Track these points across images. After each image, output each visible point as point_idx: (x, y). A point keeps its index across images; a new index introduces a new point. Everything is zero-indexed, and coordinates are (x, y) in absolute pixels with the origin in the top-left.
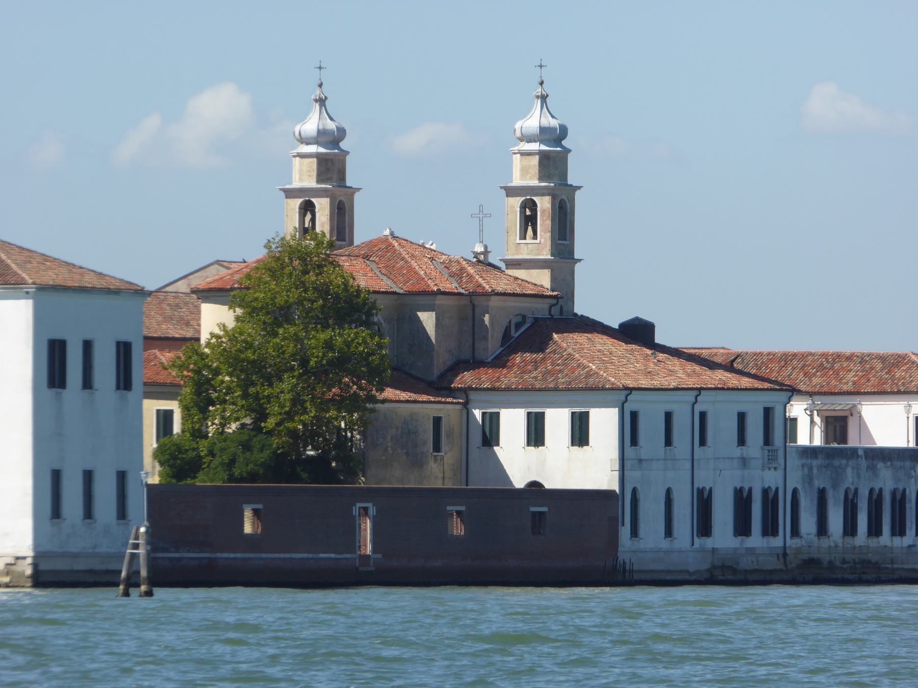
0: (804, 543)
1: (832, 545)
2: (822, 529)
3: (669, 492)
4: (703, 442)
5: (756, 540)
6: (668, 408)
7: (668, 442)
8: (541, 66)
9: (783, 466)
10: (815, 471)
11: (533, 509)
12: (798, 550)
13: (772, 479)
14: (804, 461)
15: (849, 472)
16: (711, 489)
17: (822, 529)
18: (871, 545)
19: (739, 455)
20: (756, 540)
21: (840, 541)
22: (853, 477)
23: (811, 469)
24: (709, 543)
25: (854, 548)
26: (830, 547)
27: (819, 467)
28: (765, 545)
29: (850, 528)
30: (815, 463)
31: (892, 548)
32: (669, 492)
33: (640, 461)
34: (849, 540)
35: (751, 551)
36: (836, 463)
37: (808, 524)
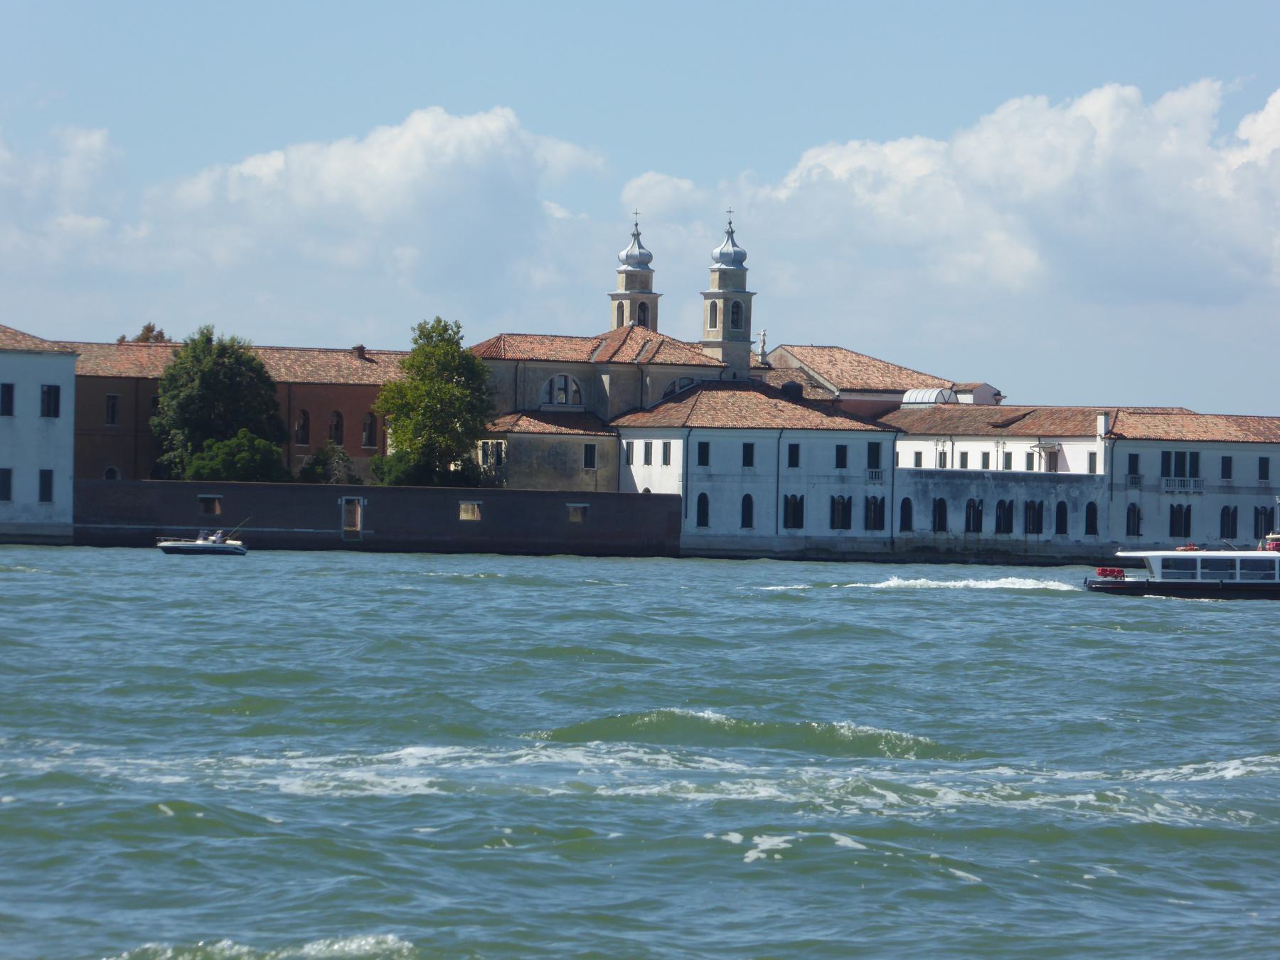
10: (931, 487)
12: (908, 541)
13: (876, 491)
21: (962, 536)
24: (800, 533)
30: (930, 481)
33: (710, 476)
35: (854, 539)
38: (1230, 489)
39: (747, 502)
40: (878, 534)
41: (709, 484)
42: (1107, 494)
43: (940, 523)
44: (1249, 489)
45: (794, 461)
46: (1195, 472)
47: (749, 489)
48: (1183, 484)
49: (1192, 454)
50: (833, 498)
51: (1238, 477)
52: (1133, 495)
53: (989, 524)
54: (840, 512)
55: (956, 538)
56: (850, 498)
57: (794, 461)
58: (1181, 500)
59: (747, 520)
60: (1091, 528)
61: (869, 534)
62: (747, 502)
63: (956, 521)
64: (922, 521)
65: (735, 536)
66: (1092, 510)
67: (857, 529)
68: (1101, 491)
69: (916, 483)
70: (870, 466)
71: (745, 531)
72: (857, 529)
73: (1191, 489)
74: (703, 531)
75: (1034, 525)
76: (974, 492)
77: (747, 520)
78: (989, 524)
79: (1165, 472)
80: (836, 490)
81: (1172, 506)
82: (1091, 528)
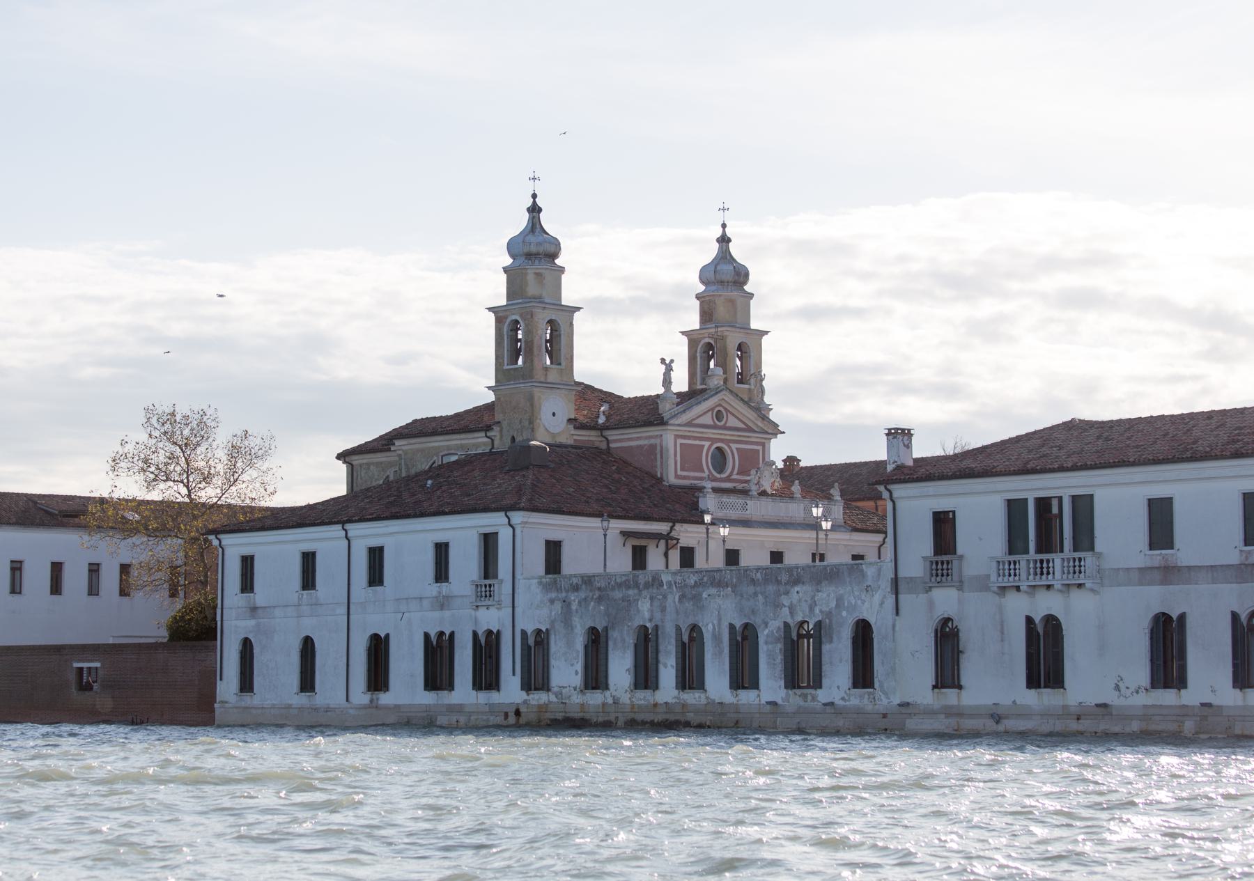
0: (553, 698)
1: (610, 701)
8: (534, 179)
10: (574, 607)
11: (76, 665)
13: (491, 618)
14: (553, 595)
19: (435, 594)
21: (625, 699)
23: (566, 603)
25: (655, 705)
26: (604, 704)
27: (584, 602)
30: (573, 597)
33: (254, 610)
36: (618, 594)
38: (1169, 574)
39: (308, 648)
40: (495, 697)
41: (253, 622)
42: (890, 600)
43: (595, 677)
44: (1215, 572)
45: (376, 577)
46: (1085, 537)
47: (308, 626)
48: (1043, 569)
49: (1075, 499)
50: (427, 636)
51: (1189, 546)
52: (946, 600)
53: (668, 674)
54: (438, 656)
55: (616, 702)
56: (452, 634)
57: (376, 577)
58: (1044, 605)
59: (307, 682)
60: (863, 676)
61: (483, 697)
62: (308, 648)
63: (620, 668)
64: (566, 672)
65: (289, 707)
66: (863, 634)
67: (463, 692)
68: (877, 597)
69: (552, 601)
70: (548, 572)
71: (303, 699)
72: (463, 692)
73: (1057, 579)
74: (247, 699)
75: (487, 677)
76: (644, 611)
77: (307, 682)
78: (668, 674)
79: (1015, 542)
80: (436, 622)
81: (1029, 620)
82: (863, 676)
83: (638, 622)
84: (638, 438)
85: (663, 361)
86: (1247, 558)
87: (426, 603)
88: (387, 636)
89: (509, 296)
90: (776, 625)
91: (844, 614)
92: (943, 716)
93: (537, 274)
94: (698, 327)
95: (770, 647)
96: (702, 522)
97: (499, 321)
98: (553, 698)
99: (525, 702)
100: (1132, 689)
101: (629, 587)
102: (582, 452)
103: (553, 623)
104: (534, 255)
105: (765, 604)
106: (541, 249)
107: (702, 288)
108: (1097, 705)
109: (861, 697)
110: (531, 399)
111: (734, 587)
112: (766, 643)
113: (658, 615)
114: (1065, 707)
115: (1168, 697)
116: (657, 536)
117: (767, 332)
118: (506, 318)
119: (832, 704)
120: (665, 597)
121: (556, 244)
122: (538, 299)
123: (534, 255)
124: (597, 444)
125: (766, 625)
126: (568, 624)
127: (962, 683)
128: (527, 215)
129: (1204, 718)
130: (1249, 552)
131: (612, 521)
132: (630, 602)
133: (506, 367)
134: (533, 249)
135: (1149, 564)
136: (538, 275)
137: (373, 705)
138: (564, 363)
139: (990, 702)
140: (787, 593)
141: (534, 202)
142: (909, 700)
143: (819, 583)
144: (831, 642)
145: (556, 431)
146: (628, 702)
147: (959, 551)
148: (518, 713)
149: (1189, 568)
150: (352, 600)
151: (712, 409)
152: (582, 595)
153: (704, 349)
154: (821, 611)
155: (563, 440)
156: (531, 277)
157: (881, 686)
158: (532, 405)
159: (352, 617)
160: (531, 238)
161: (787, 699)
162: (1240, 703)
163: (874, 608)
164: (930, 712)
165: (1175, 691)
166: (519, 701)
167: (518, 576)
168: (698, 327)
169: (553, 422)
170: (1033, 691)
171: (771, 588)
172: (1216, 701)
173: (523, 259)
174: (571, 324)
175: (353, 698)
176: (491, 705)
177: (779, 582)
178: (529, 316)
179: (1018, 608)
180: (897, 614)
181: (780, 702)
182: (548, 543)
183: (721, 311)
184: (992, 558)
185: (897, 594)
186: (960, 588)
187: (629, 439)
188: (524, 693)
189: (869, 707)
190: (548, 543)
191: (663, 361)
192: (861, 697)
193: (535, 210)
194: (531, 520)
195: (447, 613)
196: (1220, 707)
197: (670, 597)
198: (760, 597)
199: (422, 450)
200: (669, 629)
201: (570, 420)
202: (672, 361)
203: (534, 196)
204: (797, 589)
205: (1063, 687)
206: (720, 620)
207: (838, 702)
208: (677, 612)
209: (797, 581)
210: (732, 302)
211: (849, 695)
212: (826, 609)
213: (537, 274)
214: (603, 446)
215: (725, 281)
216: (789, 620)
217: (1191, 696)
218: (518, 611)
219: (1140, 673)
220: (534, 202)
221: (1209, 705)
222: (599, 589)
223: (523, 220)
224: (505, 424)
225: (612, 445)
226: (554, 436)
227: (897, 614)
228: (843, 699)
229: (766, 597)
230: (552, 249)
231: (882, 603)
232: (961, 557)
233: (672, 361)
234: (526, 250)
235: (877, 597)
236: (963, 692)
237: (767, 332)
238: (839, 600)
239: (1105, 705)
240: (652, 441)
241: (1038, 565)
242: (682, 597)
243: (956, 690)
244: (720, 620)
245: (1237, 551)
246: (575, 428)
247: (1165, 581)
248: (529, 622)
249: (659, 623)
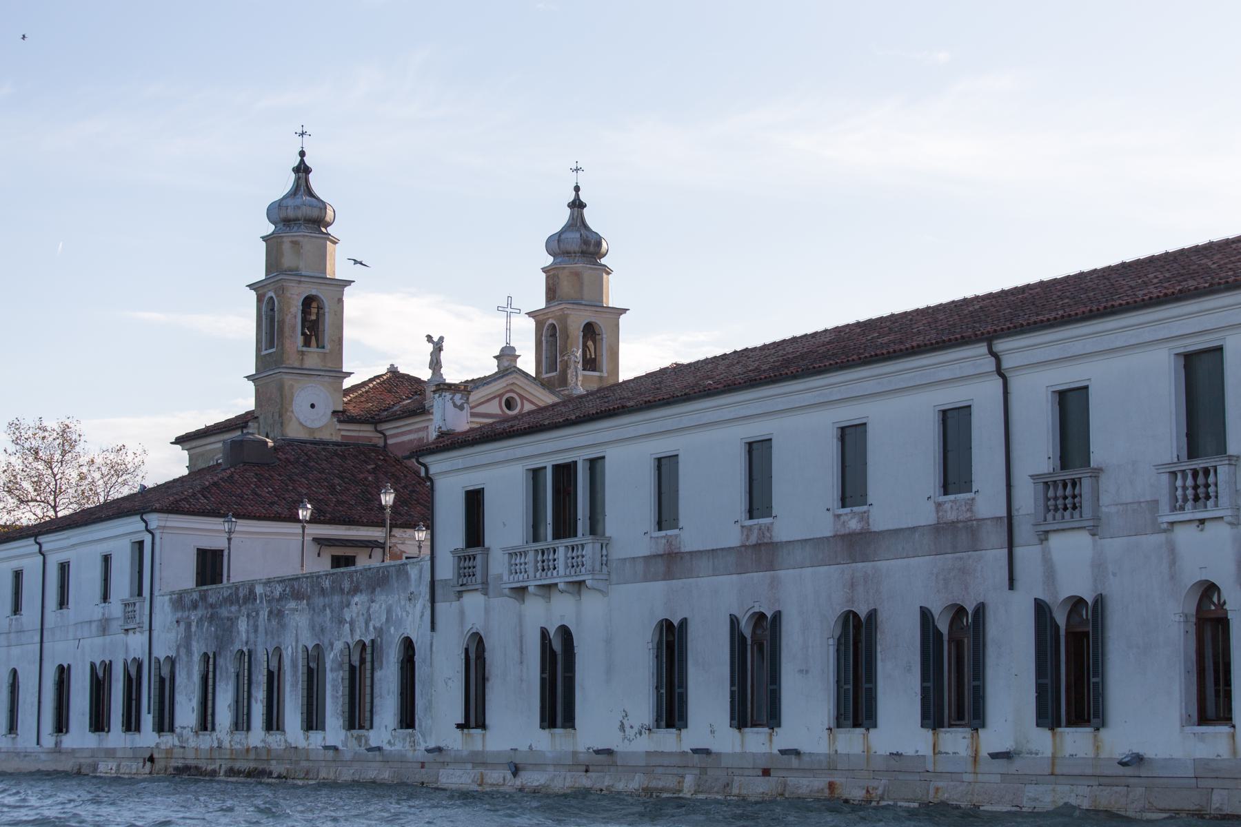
0: (177, 743)
1: (215, 745)
2: (206, 722)
3: (14, 673)
4: (63, 602)
5: (116, 737)
6: (16, 564)
7: (17, 609)
8: (302, 134)
9: (146, 626)
10: (193, 629)
12: (169, 752)
13: (136, 644)
14: (179, 614)
15: (243, 625)
16: (69, 666)
17: (206, 722)
18: (274, 746)
19: (100, 616)
20: (116, 737)
22: (248, 632)
25: (248, 750)
26: (212, 748)
27: (200, 620)
28: (129, 745)
29: (241, 722)
30: (194, 616)
31: (306, 751)
32: (14, 673)
34: (239, 736)
35: (110, 753)
36: (224, 612)
37: (186, 712)
38: (671, 563)
73: (561, 576)
83: (237, 646)
84: (410, 432)
85: (429, 338)
86: (748, 537)
87: (94, 626)
88: (69, 666)
89: (268, 271)
90: (339, 645)
91: (392, 629)
92: (469, 766)
93: (292, 242)
94: (543, 305)
95: (335, 674)
96: (294, 519)
97: (260, 299)
98: (177, 743)
99: (158, 745)
100: (636, 730)
101: (232, 604)
102: (343, 450)
103: (178, 648)
104: (300, 220)
105: (331, 618)
106: (299, 214)
107: (550, 260)
108: (598, 752)
109: (404, 739)
110: (281, 388)
111: (309, 598)
112: (332, 670)
113: (252, 636)
114: (575, 753)
115: (667, 741)
116: (370, 545)
117: (625, 311)
118: (264, 295)
119: (379, 749)
120: (257, 614)
121: (323, 206)
122: (294, 271)
123: (300, 220)
124: (375, 441)
125: (332, 645)
126: (189, 652)
127: (487, 722)
128: (293, 176)
129: (704, 770)
130: (750, 528)
131: (240, 521)
132: (233, 621)
133: (264, 353)
134: (291, 214)
135: (654, 551)
136: (295, 243)
137: (58, 750)
138: (328, 347)
139: (508, 748)
140: (348, 605)
141: (302, 161)
142: (442, 745)
143: (374, 589)
144: (381, 668)
145: (317, 425)
146: (228, 746)
147: (487, 545)
148: (151, 759)
149: (691, 553)
150: (46, 626)
151: (501, 396)
152: (200, 612)
153: (550, 334)
154: (375, 628)
155: (326, 436)
156: (287, 247)
157: (420, 726)
158: (281, 395)
159: (46, 645)
160: (290, 202)
161: (345, 744)
162: (738, 749)
163: (413, 623)
164: (459, 761)
165: (766, 730)
166: (153, 745)
167: (156, 593)
168: (543, 305)
169: (311, 414)
170: (547, 731)
171: (336, 599)
172: (715, 748)
173: (280, 226)
174: (340, 301)
175: (43, 741)
176: (134, 749)
177: (342, 590)
178: (281, 291)
179: (542, 614)
180: (433, 628)
181: (340, 747)
182: (202, 554)
183: (566, 287)
184: (504, 549)
185: (433, 601)
186: (486, 594)
187: (403, 434)
188: (155, 735)
189: (410, 754)
190: (202, 554)
191: (429, 338)
192: (404, 739)
193: (302, 170)
194: (169, 524)
195: (108, 638)
196: (718, 755)
197: (261, 613)
198: (328, 611)
199: (202, 455)
200: (261, 656)
201: (334, 413)
202: (441, 339)
203: (302, 154)
204: (356, 599)
205: (573, 727)
206: (297, 642)
207: (387, 747)
208: (266, 633)
209: (356, 590)
210: (577, 275)
211: (394, 737)
212: (378, 625)
213: (292, 242)
214: (381, 443)
215: (577, 252)
216: (350, 641)
217: (785, 737)
218: (155, 634)
219: (643, 708)
220: (302, 161)
221: (707, 752)
222: (211, 605)
223: (287, 182)
224: (261, 419)
225: (390, 442)
226: (312, 431)
227: (433, 628)
228: (389, 742)
229: (332, 611)
230: (315, 213)
231: (422, 616)
232: (488, 549)
233: (441, 339)
234: (283, 214)
235: (419, 607)
236: (488, 733)
237: (625, 311)
238: (389, 611)
239: (609, 752)
240: (421, 434)
241: (539, 558)
242: (270, 612)
243: (479, 731)
244: (297, 642)
245: (738, 527)
246: (340, 421)
247: (668, 575)
248: (161, 652)
249: (252, 647)
